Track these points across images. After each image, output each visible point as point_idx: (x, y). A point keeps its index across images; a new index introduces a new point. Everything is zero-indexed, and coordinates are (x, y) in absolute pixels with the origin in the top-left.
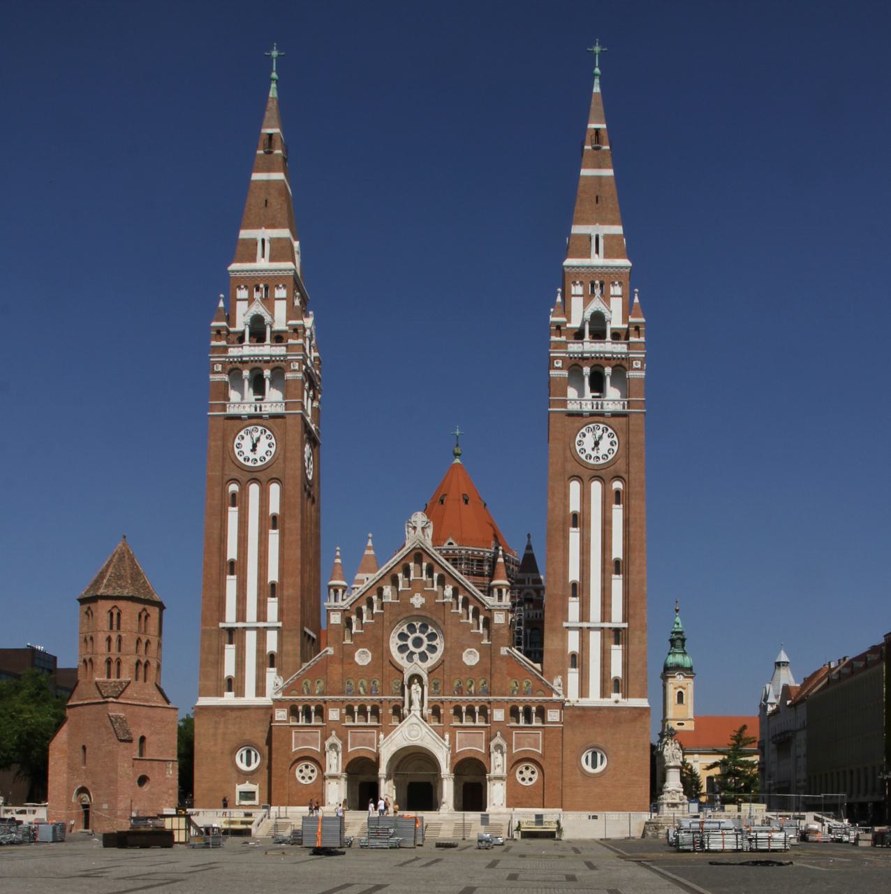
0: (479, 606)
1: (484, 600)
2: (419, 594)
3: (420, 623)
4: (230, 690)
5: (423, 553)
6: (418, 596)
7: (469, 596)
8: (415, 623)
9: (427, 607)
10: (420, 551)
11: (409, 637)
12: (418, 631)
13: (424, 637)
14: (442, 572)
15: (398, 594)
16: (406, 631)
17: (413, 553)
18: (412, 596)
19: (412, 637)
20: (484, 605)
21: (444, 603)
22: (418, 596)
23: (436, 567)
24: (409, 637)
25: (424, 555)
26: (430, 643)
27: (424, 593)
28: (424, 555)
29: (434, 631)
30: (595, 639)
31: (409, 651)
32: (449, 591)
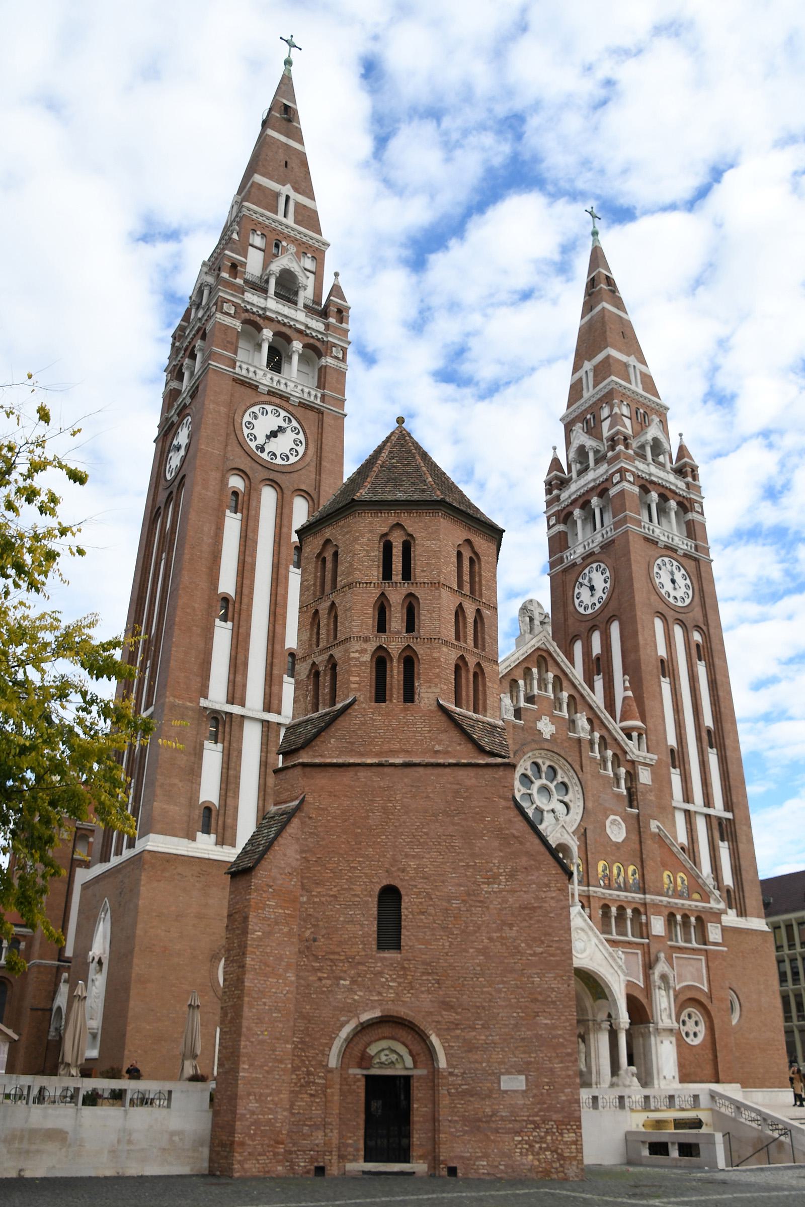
0: (619, 752)
1: (627, 745)
2: (548, 718)
3: (548, 763)
4: (207, 830)
5: (549, 659)
6: (545, 720)
7: (606, 736)
8: (540, 761)
9: (559, 741)
10: (544, 654)
11: (552, 782)
12: (543, 775)
13: (552, 786)
14: (573, 692)
15: (518, 713)
16: (529, 773)
17: (536, 655)
18: (539, 719)
19: (538, 783)
20: (625, 753)
21: (579, 740)
22: (545, 720)
23: (565, 684)
24: (532, 782)
25: (550, 662)
26: (561, 798)
27: (554, 719)
28: (550, 662)
29: (566, 780)
30: (701, 825)
31: (534, 806)
32: (582, 721)
